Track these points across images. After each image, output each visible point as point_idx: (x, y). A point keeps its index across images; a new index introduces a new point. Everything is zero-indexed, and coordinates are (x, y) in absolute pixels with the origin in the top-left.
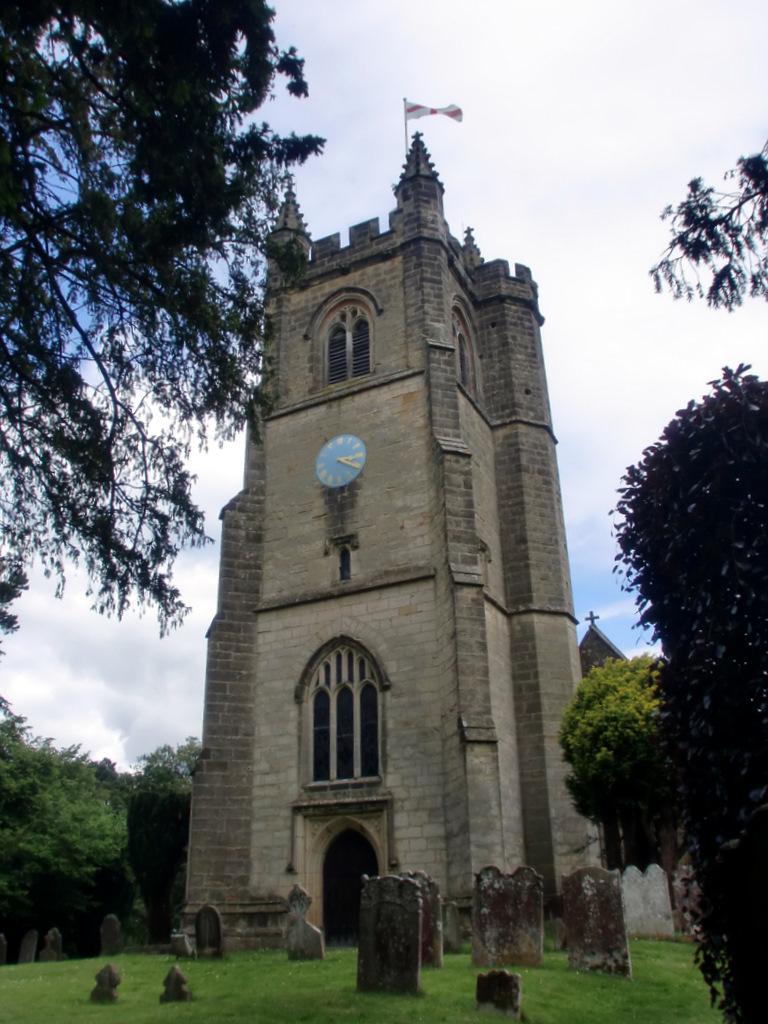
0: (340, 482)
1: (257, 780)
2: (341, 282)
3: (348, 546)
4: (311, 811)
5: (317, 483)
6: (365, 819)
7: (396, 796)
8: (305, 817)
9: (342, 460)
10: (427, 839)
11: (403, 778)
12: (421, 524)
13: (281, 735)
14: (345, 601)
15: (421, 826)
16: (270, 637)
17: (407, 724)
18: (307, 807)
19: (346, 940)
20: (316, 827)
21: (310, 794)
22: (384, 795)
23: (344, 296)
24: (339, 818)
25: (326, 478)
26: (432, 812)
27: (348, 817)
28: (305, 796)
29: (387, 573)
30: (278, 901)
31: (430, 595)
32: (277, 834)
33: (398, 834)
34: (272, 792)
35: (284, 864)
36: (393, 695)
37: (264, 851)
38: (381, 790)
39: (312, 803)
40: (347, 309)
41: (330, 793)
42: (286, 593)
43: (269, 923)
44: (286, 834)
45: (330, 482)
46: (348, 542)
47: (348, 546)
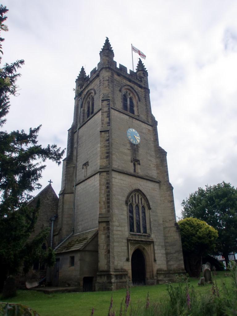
0: (134, 142)
1: (115, 228)
2: (129, 83)
3: (136, 163)
4: (132, 242)
5: (128, 139)
6: (145, 246)
7: (154, 241)
8: (130, 243)
9: (135, 136)
10: (162, 254)
11: (155, 236)
12: (154, 167)
13: (122, 215)
14: (138, 179)
15: (160, 250)
16: (117, 180)
17: (155, 221)
18: (132, 240)
19: (136, 283)
20: (131, 247)
21: (132, 236)
22: (151, 240)
23: (129, 88)
24: (139, 245)
25: (133, 141)
26: (162, 246)
27: (142, 245)
28: (130, 236)
29: (147, 176)
30: (124, 270)
31: (158, 187)
32: (123, 248)
33: (156, 252)
34: (119, 233)
35: (125, 258)
36: (151, 211)
37: (119, 253)
38: (150, 238)
39: (134, 239)
40: (129, 92)
41: (138, 237)
42: (120, 168)
43: (123, 278)
44: (126, 248)
45: (132, 140)
46: (137, 162)
47: (136, 163)
